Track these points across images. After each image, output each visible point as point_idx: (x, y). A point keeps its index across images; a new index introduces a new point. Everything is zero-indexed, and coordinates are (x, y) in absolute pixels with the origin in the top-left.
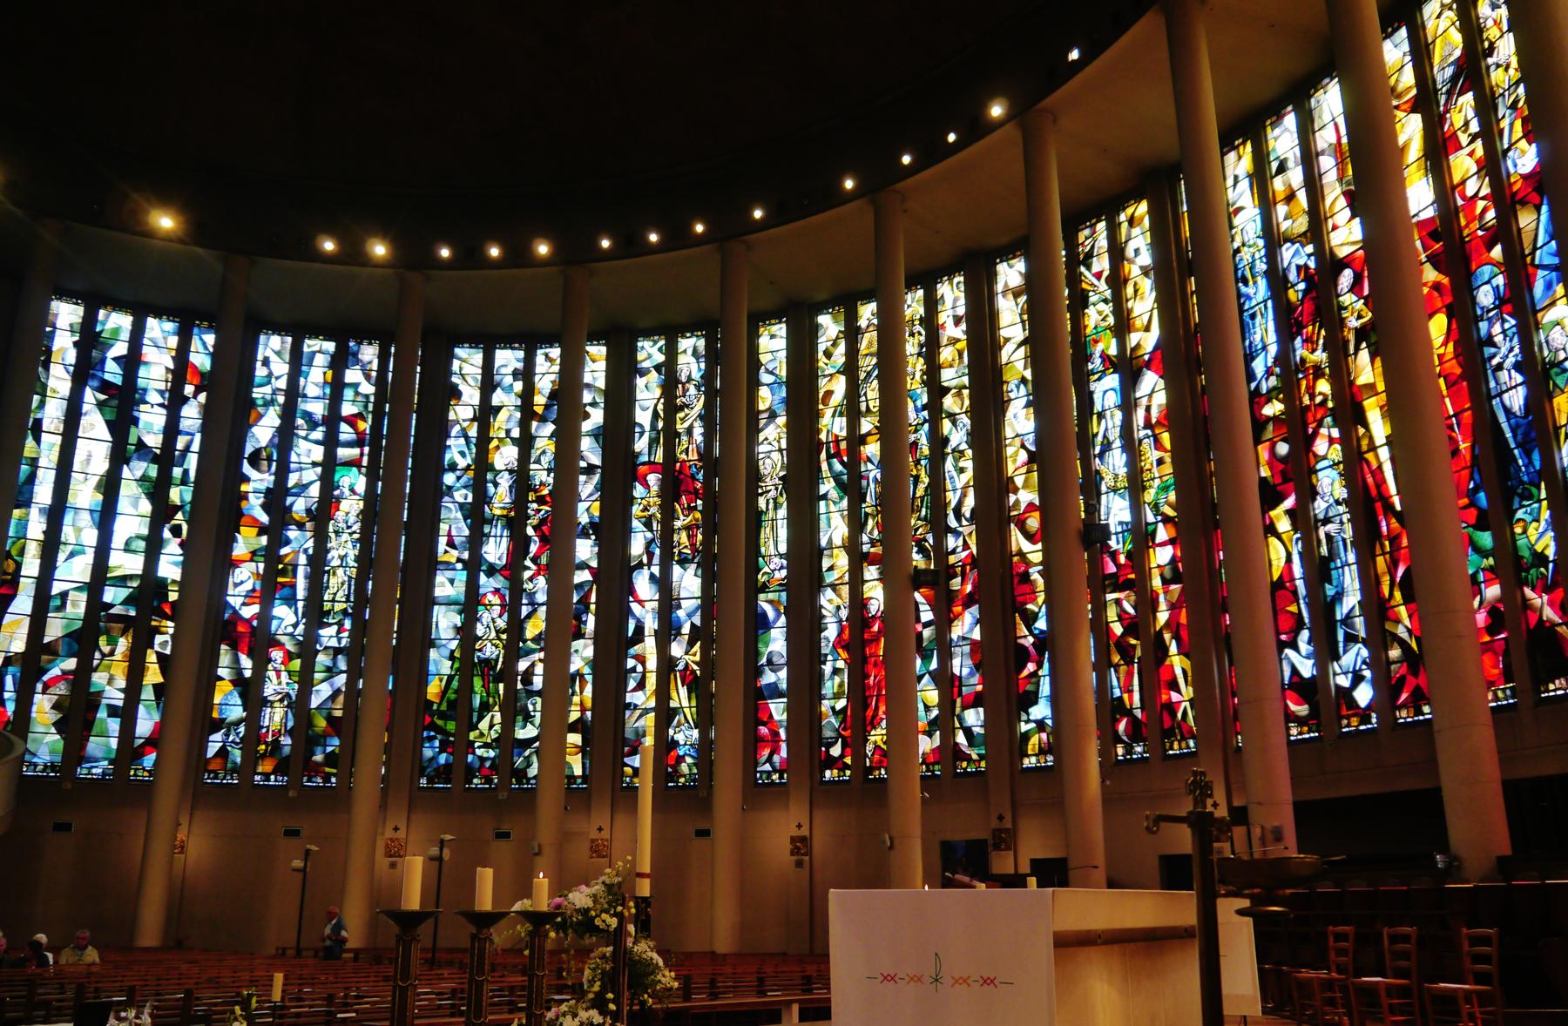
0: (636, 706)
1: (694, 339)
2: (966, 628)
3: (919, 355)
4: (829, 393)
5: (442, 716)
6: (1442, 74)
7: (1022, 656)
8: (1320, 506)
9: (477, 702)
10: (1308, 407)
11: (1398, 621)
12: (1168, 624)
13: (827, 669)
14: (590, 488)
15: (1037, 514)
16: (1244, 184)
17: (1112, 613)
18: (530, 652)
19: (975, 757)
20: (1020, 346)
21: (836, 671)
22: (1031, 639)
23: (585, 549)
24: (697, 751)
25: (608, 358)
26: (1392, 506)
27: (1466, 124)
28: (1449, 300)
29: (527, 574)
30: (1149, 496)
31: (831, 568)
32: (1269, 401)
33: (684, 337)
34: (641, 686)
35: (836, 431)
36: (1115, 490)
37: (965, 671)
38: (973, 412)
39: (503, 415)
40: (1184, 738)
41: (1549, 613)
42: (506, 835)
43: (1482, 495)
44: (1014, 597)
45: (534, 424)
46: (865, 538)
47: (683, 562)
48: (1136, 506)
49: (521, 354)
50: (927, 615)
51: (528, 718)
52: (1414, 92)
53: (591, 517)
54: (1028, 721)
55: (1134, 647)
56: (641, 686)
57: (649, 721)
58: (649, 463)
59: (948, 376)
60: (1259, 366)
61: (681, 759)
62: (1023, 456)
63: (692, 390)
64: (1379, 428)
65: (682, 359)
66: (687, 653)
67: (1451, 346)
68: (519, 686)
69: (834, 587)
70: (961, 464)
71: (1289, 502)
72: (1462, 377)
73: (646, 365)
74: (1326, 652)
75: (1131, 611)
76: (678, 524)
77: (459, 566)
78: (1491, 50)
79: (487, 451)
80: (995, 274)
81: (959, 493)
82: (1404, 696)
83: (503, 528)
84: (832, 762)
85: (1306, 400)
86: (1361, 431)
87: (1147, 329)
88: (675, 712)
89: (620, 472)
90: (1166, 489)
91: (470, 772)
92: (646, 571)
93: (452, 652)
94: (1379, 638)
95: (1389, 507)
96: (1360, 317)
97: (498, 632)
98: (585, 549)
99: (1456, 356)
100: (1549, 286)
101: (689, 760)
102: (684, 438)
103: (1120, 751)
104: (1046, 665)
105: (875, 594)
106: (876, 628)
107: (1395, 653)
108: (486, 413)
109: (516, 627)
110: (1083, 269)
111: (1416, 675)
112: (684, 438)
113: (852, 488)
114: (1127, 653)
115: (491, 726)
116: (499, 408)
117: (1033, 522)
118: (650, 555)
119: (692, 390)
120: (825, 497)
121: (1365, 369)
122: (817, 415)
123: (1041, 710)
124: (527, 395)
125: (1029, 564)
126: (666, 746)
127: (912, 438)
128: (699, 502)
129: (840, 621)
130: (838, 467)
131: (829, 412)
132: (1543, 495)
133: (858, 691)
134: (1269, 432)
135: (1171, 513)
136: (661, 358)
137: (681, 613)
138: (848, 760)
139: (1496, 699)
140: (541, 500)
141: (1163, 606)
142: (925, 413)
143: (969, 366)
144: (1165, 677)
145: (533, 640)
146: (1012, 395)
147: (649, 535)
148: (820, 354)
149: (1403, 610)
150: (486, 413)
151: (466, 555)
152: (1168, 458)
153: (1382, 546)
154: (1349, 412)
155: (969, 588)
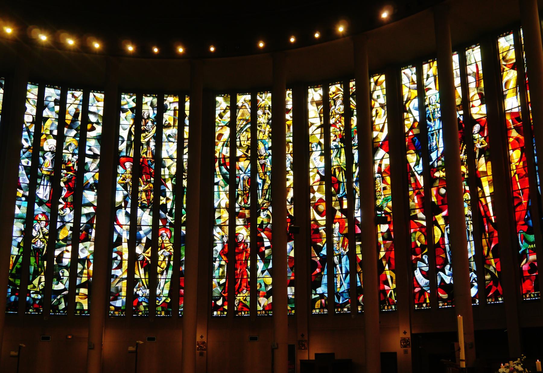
0: (117, 277)
1: (151, 98)
3: (268, 123)
4: (221, 135)
5: (13, 276)
7: (314, 265)
9: (32, 269)
11: (490, 265)
12: (384, 257)
13: (216, 264)
14: (95, 165)
15: (324, 204)
16: (432, 79)
18: (61, 246)
20: (318, 128)
21: (220, 266)
22: (318, 258)
23: (90, 196)
24: (148, 300)
25: (105, 100)
28: (522, 145)
29: (60, 206)
31: (219, 218)
32: (438, 170)
33: (146, 96)
34: (120, 267)
35: (224, 153)
39: (48, 123)
40: (390, 305)
42: (48, 338)
43: (530, 221)
44: (311, 239)
45: (66, 129)
46: (237, 205)
47: (143, 207)
49: (59, 92)
50: (267, 244)
51: (60, 280)
52: (514, 61)
53: (95, 180)
54: (316, 294)
56: (120, 267)
57: (123, 285)
58: (126, 156)
60: (434, 156)
61: (140, 303)
62: (318, 177)
63: (150, 123)
64: (488, 190)
65: (144, 107)
66: (144, 252)
67: (521, 163)
68: (55, 263)
69: (221, 226)
71: (445, 213)
72: (525, 176)
73: (126, 107)
76: (141, 189)
77: (24, 199)
79: (40, 140)
80: (307, 93)
82: (490, 294)
83: (48, 181)
84: (217, 308)
86: (479, 189)
87: (382, 131)
88: (137, 280)
89: (110, 159)
90: (387, 200)
91: (28, 305)
92: (123, 210)
93: (19, 243)
94: (481, 271)
95: (489, 220)
96: (482, 144)
97: (44, 235)
98: (90, 196)
99: (524, 167)
101: (144, 304)
102: (145, 147)
104: (326, 270)
105: (243, 233)
106: (241, 247)
107: (488, 277)
108: (39, 120)
109: (53, 233)
111: (496, 285)
112: (145, 147)
113: (231, 180)
115: (40, 283)
116: (47, 119)
117: (322, 207)
118: (126, 203)
119: (150, 123)
120: (217, 184)
121: (483, 165)
122: (214, 144)
123: (322, 289)
124: (62, 113)
125: (319, 225)
126: (131, 296)
127: (263, 161)
128: (152, 179)
129: (223, 243)
130: (224, 170)
131: (220, 144)
133: (231, 274)
134: (437, 183)
135: (389, 211)
136: (134, 105)
137: (141, 233)
138: (226, 307)
139: (530, 297)
140: (68, 169)
141: (383, 249)
142: (270, 151)
143: (293, 133)
144: (382, 279)
145: (63, 240)
146: (314, 149)
147: (125, 192)
148: (217, 116)
150: (39, 120)
151: (27, 194)
152: (388, 187)
153: (485, 235)
154: (475, 180)
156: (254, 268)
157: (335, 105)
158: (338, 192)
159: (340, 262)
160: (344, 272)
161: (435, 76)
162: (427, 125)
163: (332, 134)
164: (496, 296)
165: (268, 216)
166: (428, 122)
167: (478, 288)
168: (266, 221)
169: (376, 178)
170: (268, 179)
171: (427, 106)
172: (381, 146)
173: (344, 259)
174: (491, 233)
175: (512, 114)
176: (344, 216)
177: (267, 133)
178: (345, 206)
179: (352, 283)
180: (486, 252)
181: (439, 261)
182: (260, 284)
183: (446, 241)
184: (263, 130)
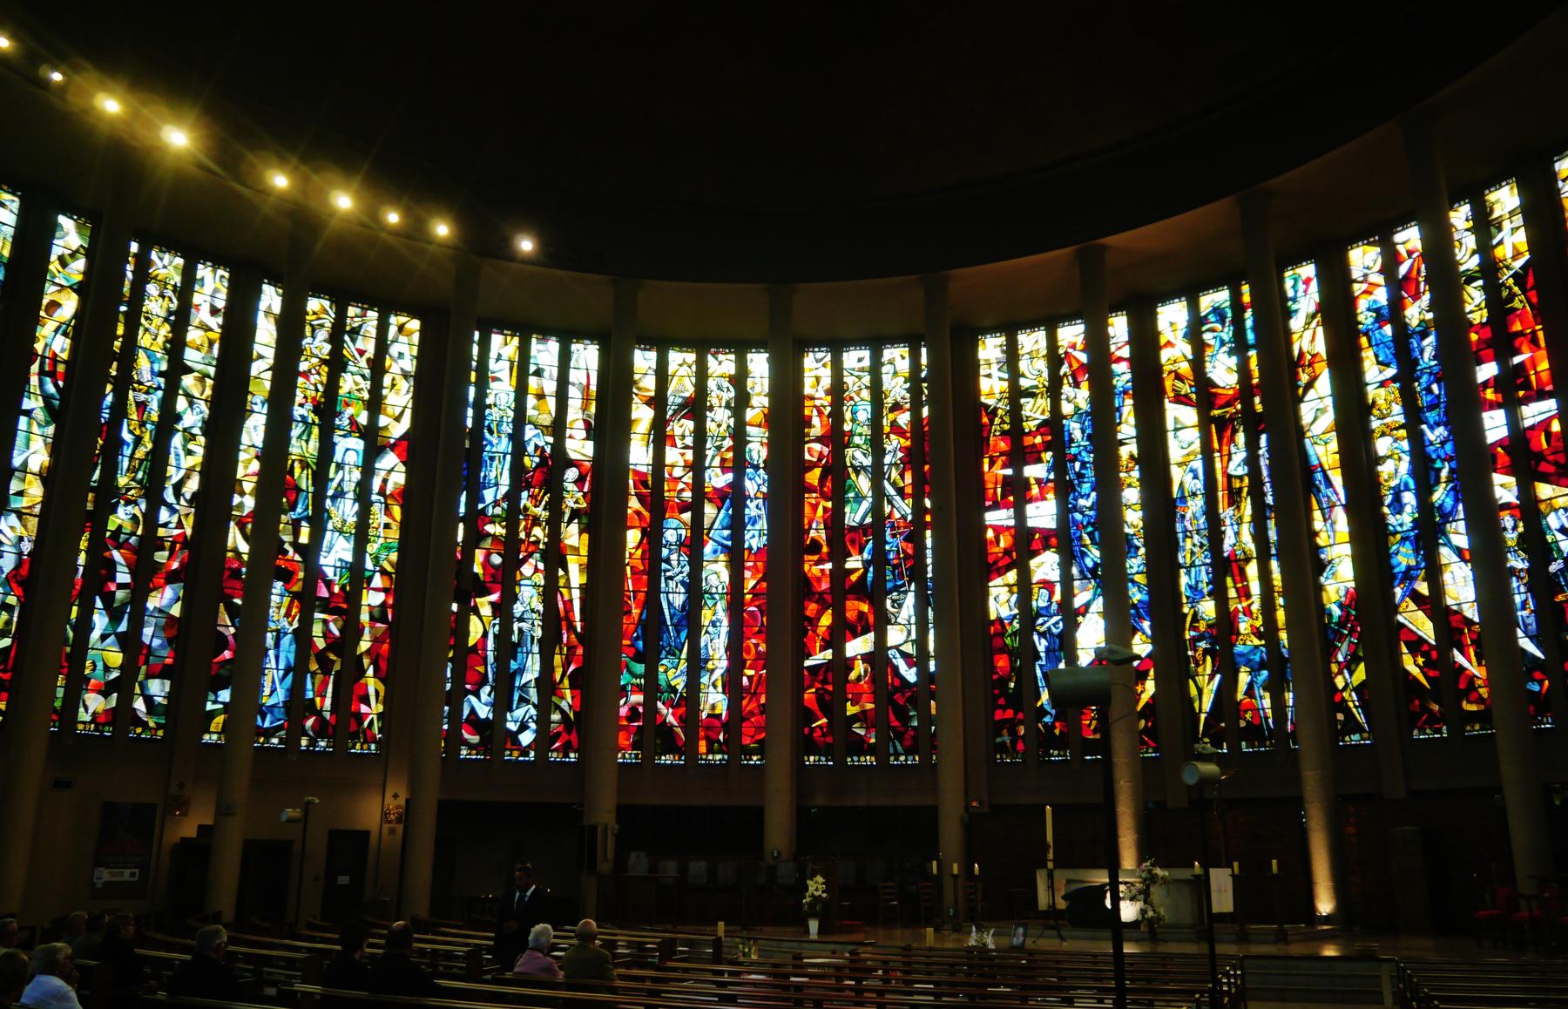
2: (165, 602)
3: (166, 320)
4: (54, 305)
6: (673, 400)
8: (518, 609)
10: (523, 541)
11: (563, 698)
12: (368, 652)
17: (317, 630)
19: (152, 724)
26: (575, 628)
27: (683, 437)
30: (372, 548)
31: (20, 494)
35: (56, 347)
36: (341, 532)
37: (156, 642)
38: (213, 403)
40: (366, 741)
41: (671, 719)
48: (359, 551)
50: (123, 577)
54: (215, 702)
55: (333, 662)
59: (191, 356)
60: (489, 495)
64: (576, 575)
69: (20, 514)
70: (191, 446)
71: (494, 597)
72: (643, 572)
74: (502, 704)
75: (337, 633)
78: (711, 408)
80: (260, 291)
81: (182, 472)
85: (522, 535)
86: (561, 572)
87: (398, 419)
90: (389, 549)
94: (544, 708)
95: (571, 628)
99: (642, 558)
100: (715, 552)
103: (304, 742)
107: (556, 717)
110: (346, 338)
111: (569, 733)
114: (326, 667)
120: (28, 413)
121: (572, 535)
122: (36, 321)
127: (142, 397)
129: (20, 554)
130: (51, 389)
132: (684, 655)
134: (488, 543)
135: (390, 569)
141: (367, 636)
144: (358, 692)
146: (256, 408)
148: (53, 258)
149: (568, 693)
152: (395, 526)
154: (555, 557)
155: (175, 565)
156: (84, 626)
157: (313, 337)
158: (293, 508)
159: (277, 645)
160: (282, 665)
161: (512, 362)
162: (484, 438)
163: (298, 392)
164: (565, 750)
165: (134, 517)
166: (487, 435)
167: (536, 731)
168: (128, 528)
169: (372, 503)
170: (147, 437)
171: (490, 406)
172: (393, 447)
173: (286, 641)
174: (571, 648)
175: (636, 473)
176: (297, 558)
177: (161, 340)
178: (304, 538)
179: (296, 691)
180: (558, 677)
181: (469, 675)
182: (94, 664)
183: (490, 644)
184: (153, 328)
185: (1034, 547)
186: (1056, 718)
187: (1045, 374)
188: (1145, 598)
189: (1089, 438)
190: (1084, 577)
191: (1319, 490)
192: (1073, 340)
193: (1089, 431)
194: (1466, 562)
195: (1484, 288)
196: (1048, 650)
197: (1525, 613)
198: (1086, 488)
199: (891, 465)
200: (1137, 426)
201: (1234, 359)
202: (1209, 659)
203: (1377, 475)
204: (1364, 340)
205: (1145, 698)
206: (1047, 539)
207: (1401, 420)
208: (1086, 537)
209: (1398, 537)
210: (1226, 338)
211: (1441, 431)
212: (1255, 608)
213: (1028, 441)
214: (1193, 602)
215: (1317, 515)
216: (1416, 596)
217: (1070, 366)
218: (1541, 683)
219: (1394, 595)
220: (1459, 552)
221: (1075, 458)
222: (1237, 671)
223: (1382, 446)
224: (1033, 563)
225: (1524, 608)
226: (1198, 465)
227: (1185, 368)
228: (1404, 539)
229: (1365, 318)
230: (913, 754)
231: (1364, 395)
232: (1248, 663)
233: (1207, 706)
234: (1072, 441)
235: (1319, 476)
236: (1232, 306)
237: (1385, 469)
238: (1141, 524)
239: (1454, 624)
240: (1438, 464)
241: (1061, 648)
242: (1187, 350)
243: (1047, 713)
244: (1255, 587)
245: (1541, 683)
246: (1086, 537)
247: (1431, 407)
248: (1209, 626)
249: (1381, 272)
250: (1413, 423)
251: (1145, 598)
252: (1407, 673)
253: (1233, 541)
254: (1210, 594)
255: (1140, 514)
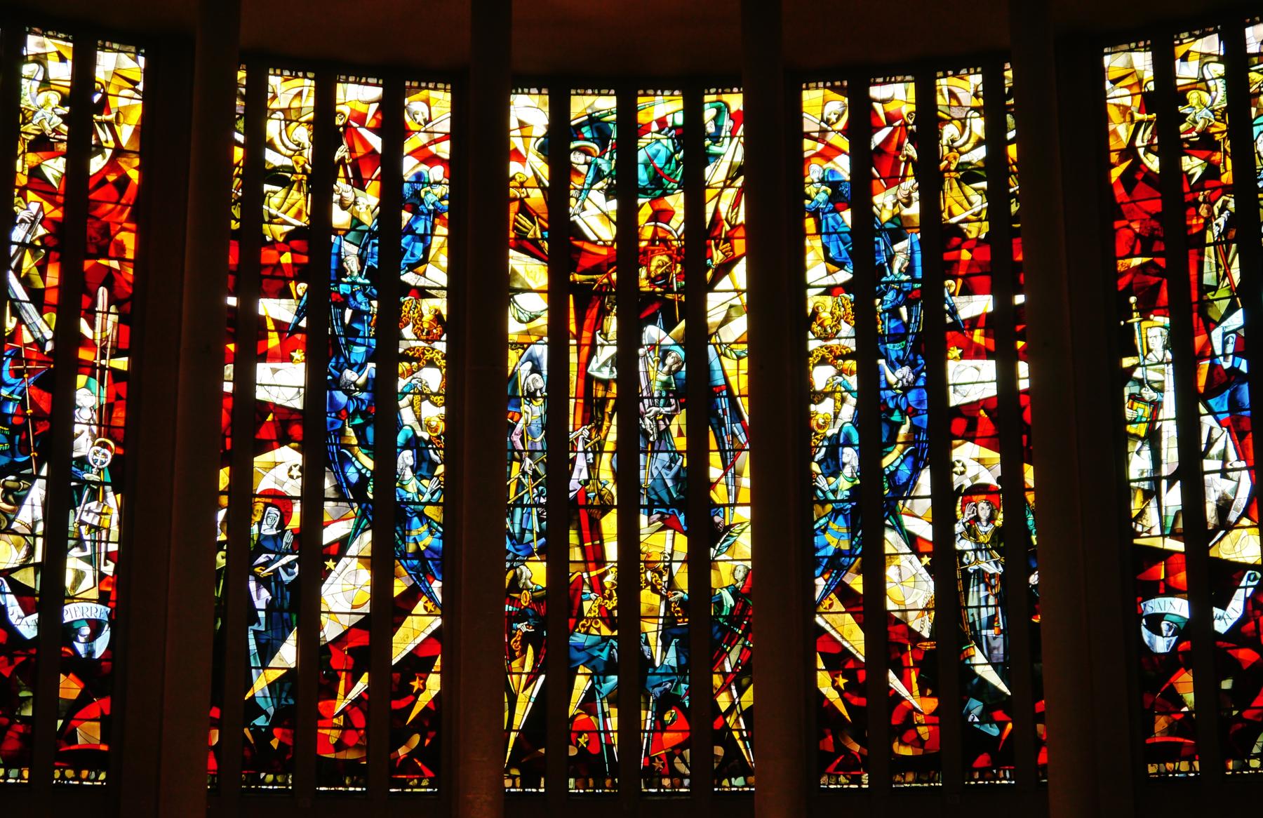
185: (263, 434)
186: (277, 720)
187: (308, 153)
188: (438, 544)
189: (371, 274)
190: (341, 498)
191: (721, 423)
192: (362, 108)
193: (372, 262)
194: (920, 556)
195: (988, 194)
196: (270, 607)
197: (991, 633)
198: (358, 353)
199: (23, 245)
200: (451, 272)
201: (613, 205)
202: (530, 648)
203: (808, 416)
204: (810, 224)
205: (424, 700)
206: (286, 426)
207: (851, 345)
208: (350, 432)
209: (829, 507)
210: (605, 168)
211: (905, 372)
212: (609, 580)
213: (268, 256)
214: (518, 561)
215: (715, 458)
216: (845, 594)
217: (352, 149)
218: (1002, 727)
219: (814, 587)
220: (912, 540)
221: (344, 302)
222: (574, 673)
223: (821, 377)
224: (260, 461)
225: (990, 625)
226: (541, 351)
227: (536, 197)
228: (836, 513)
229: (817, 194)
230: (19, 767)
231: (803, 300)
232: (590, 661)
233: (519, 720)
234: (342, 272)
235: (724, 403)
236: (618, 122)
237: (822, 410)
238: (442, 426)
239: (893, 637)
240: (896, 417)
241: (293, 608)
242: (544, 170)
243: (260, 712)
244: (611, 551)
245: (1002, 727)
246: (350, 432)
247: (895, 337)
248: (535, 600)
249: (845, 132)
250: (868, 351)
251: (438, 544)
252: (823, 696)
253: (585, 476)
254: (541, 551)
255: (443, 410)
